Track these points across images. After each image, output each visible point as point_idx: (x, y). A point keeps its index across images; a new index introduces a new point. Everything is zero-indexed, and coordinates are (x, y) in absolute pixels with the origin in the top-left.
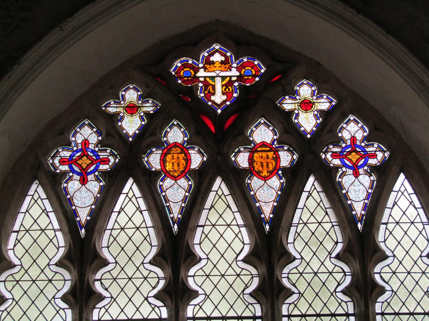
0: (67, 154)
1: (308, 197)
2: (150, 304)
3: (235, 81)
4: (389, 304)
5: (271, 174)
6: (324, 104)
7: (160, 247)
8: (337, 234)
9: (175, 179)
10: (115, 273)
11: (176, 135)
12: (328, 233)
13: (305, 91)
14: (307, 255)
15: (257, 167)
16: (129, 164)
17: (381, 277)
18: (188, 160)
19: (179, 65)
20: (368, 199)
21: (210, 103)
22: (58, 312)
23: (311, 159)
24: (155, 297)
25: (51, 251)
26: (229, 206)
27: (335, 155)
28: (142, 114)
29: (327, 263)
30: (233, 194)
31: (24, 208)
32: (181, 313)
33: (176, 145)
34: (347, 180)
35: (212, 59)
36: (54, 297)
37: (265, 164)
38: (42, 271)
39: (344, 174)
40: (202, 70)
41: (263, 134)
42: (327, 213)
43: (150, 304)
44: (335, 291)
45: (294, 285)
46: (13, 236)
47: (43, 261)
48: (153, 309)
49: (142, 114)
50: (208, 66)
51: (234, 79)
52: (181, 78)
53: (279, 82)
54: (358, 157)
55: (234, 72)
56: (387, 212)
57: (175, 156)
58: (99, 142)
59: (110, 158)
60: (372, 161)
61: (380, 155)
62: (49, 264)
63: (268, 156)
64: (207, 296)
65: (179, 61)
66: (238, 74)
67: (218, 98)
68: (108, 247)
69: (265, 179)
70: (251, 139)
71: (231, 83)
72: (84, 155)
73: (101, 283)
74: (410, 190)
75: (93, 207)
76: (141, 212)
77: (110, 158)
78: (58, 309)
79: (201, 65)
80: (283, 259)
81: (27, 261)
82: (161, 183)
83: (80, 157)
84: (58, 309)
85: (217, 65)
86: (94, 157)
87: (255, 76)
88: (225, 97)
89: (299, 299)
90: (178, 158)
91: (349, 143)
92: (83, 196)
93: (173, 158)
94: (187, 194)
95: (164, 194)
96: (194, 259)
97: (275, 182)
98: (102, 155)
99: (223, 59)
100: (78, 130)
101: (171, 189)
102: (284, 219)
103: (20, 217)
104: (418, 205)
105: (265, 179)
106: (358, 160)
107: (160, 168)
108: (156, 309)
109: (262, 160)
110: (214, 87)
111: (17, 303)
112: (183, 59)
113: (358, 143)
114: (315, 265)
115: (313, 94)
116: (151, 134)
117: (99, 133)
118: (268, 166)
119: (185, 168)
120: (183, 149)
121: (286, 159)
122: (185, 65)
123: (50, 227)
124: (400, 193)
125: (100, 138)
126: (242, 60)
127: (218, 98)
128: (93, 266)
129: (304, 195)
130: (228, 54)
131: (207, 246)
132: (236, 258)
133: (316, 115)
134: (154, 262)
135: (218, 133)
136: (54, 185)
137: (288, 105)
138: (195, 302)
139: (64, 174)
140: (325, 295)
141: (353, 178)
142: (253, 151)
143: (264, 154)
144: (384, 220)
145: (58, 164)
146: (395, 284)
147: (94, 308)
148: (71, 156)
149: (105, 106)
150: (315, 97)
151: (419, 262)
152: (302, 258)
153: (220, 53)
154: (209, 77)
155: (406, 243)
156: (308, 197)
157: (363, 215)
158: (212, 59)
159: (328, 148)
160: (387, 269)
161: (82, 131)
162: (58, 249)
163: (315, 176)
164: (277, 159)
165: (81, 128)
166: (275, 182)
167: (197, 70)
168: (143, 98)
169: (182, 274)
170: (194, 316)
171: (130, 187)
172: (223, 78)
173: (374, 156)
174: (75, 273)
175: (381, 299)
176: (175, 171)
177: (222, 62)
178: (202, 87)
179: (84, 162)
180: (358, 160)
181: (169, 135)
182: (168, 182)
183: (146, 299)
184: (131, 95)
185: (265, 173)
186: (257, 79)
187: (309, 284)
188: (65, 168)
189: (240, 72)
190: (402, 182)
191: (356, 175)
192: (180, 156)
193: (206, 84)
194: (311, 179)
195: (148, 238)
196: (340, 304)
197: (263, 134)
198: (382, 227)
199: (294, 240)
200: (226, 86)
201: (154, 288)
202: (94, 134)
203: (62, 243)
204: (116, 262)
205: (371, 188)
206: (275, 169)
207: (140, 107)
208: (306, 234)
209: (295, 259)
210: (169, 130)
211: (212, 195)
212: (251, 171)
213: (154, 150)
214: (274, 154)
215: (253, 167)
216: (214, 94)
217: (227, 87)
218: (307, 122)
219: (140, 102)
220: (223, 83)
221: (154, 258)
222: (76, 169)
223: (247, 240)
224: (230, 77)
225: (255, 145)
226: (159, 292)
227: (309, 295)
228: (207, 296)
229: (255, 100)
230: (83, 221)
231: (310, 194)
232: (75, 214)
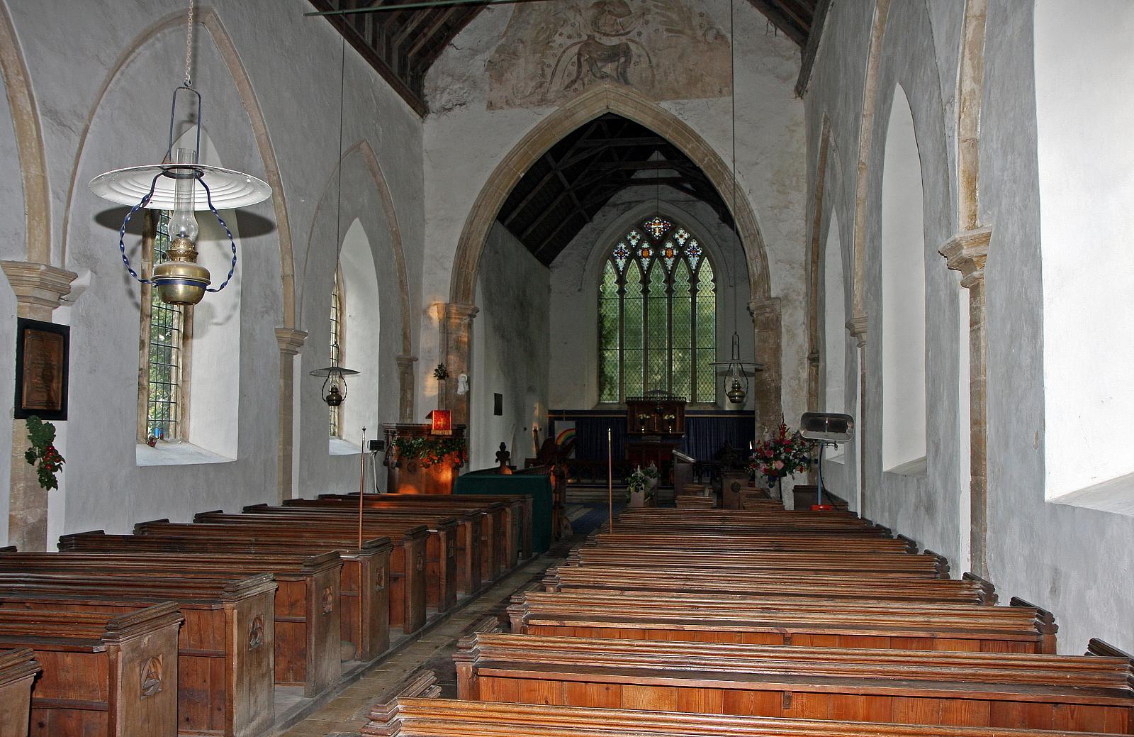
6: (686, 236)
11: (646, 245)
13: (681, 232)
16: (633, 255)
23: (682, 254)
41: (669, 245)
53: (674, 229)
92: (621, 263)
96: (650, 282)
97: (672, 259)
120: (648, 249)
135: (657, 244)
137: (677, 236)
142: (666, 250)
166: (672, 259)
168: (637, 234)
171: (634, 261)
184: (634, 233)
218: (681, 241)
229: (667, 235)
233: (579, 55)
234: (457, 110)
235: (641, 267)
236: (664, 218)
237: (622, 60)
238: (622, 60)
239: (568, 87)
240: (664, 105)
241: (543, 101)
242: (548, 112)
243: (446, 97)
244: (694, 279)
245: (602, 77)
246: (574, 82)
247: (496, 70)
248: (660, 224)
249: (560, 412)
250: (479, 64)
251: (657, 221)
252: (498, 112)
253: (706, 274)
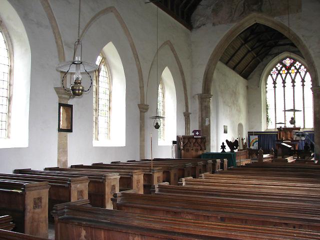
6: (300, 64)
41: (293, 68)
53: (294, 63)
92: (274, 76)
116: (281, 69)
135: (288, 69)
136: (271, 75)
137: (295, 65)
184: (279, 65)
229: (292, 65)
233: (244, 4)
234: (203, 27)
235: (282, 77)
236: (290, 58)
237: (260, 4)
238: (260, 4)
239: (241, 15)
240: (275, 18)
241: (232, 21)
242: (234, 25)
243: (198, 23)
245: (253, 11)
246: (243, 13)
247: (215, 12)
249: (252, 132)
250: (209, 11)
252: (216, 26)
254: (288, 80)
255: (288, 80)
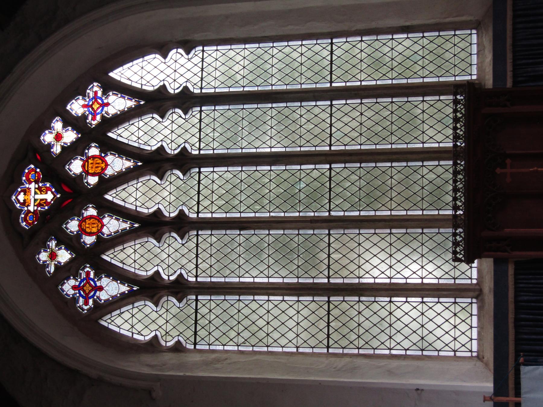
0: (81, 301)
1: (121, 136)
2: (186, 242)
3: (39, 186)
4: (195, 84)
5: (104, 160)
6: (58, 125)
7: (146, 298)
8: (147, 118)
9: (103, 225)
10: (165, 266)
12: (146, 124)
13: (48, 138)
14: (160, 137)
15: (99, 170)
17: (177, 89)
18: (91, 217)
19: (24, 223)
20: (125, 97)
21: (52, 202)
22: (189, 305)
24: (182, 239)
25: (147, 310)
26: (124, 189)
27: (94, 119)
28: (57, 249)
29: (166, 124)
30: (115, 187)
31: (117, 329)
32: (195, 220)
33: (80, 226)
34: (111, 111)
35: (22, 201)
36: (179, 308)
37: (97, 165)
38: (160, 316)
39: (107, 113)
40: (29, 208)
41: (76, 167)
42: (132, 124)
43: (186, 242)
44: (184, 119)
45: (179, 146)
46: (135, 336)
47: (154, 316)
48: (190, 240)
49: (57, 249)
50: (27, 204)
51: (37, 186)
52: (33, 222)
54: (96, 103)
55: (33, 186)
56: (134, 84)
57: (87, 226)
58: (74, 278)
59: (86, 270)
60: (100, 94)
61: (96, 89)
62: (156, 312)
63: (92, 163)
64: (186, 142)
65: (22, 224)
66: (33, 183)
67: (49, 197)
68: (147, 271)
69: (107, 165)
70: (75, 233)
71: (39, 188)
72: (83, 288)
73: (171, 275)
74: (120, 69)
75: (119, 282)
76: (124, 249)
77: (86, 270)
78: (187, 305)
79: (26, 209)
80: (161, 152)
81: (153, 327)
82: (106, 235)
83: (93, 109)
84: (187, 305)
85: (26, 197)
86: (85, 282)
87: (36, 172)
88: (49, 192)
89: (188, 143)
90: (89, 224)
91: (86, 109)
93: (89, 227)
94: (114, 218)
95: (113, 234)
96: (158, 212)
97: (109, 159)
98: (84, 275)
99: (22, 193)
100: (65, 293)
101: (110, 229)
102: (135, 151)
103: (122, 332)
104: (131, 64)
105: (107, 165)
106: (98, 103)
107: (95, 237)
108: (190, 238)
109: (94, 167)
110: (41, 200)
111: (181, 333)
112: (20, 221)
113: (86, 103)
114: (167, 132)
115: (51, 133)
116: (71, 242)
117: (68, 279)
118: (98, 163)
119: (96, 219)
121: (94, 151)
122: (25, 219)
123: (131, 311)
124: (122, 76)
125: (72, 278)
126: (24, 180)
127: (49, 197)
128: (159, 280)
129: (120, 139)
130: (19, 190)
131: (149, 204)
132: (159, 184)
133: (66, 131)
134: (165, 56)
137: (57, 149)
138: (189, 149)
139: (94, 301)
140: (187, 126)
141: (110, 107)
142: (88, 173)
143: (90, 166)
144: (139, 86)
145: (88, 307)
146: (182, 80)
147: (187, 280)
148: (83, 297)
149: (50, 273)
150: (53, 132)
151: (169, 64)
152: (162, 141)
153: (18, 196)
154: (34, 203)
155: (155, 72)
156: (121, 136)
157: (135, 101)
158: (22, 201)
159: (88, 123)
160: (172, 85)
161: (66, 290)
162: (146, 305)
163: (109, 72)
164: (94, 157)
165: (63, 291)
166: (109, 159)
167: (29, 211)
169: (167, 219)
170: (196, 213)
172: (36, 193)
173: (96, 93)
174: (163, 293)
175: (191, 89)
176: (98, 226)
177: (25, 194)
178: (41, 208)
179: (87, 288)
180: (98, 103)
181: (73, 230)
182: (105, 230)
183: (183, 245)
185: (103, 165)
186: (38, 170)
187: (179, 136)
188: (91, 302)
189: (32, 182)
190: (115, 75)
191: (108, 104)
192: (87, 223)
193: (39, 205)
194: (110, 134)
195: (142, 244)
196: (194, 116)
197: (76, 167)
198: (144, 87)
199: (149, 145)
200: (41, 191)
201: (176, 240)
202: (69, 282)
203: (142, 303)
204: (157, 265)
205: (117, 94)
206: (100, 159)
207: (52, 250)
208: (146, 138)
209: (162, 146)
210: (69, 230)
211: (116, 201)
212: (100, 175)
213: (82, 240)
214: (90, 159)
215: (98, 173)
216: (46, 200)
217: (42, 191)
218: (70, 136)
219: (48, 250)
220: (39, 193)
221: (156, 239)
222: (92, 294)
223: (148, 178)
224: (35, 188)
225: (83, 172)
226: (179, 236)
227: (187, 136)
228: (182, 267)
230: (128, 289)
231: (119, 135)
232: (123, 294)
244: (156, 102)
248: (26, 192)
251: (21, 197)
253: (145, 72)
254: (142, 196)
255: (142, 196)
